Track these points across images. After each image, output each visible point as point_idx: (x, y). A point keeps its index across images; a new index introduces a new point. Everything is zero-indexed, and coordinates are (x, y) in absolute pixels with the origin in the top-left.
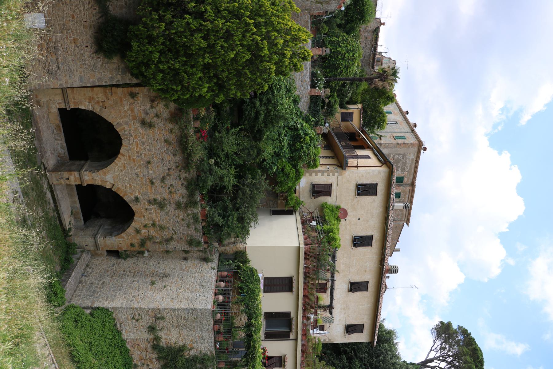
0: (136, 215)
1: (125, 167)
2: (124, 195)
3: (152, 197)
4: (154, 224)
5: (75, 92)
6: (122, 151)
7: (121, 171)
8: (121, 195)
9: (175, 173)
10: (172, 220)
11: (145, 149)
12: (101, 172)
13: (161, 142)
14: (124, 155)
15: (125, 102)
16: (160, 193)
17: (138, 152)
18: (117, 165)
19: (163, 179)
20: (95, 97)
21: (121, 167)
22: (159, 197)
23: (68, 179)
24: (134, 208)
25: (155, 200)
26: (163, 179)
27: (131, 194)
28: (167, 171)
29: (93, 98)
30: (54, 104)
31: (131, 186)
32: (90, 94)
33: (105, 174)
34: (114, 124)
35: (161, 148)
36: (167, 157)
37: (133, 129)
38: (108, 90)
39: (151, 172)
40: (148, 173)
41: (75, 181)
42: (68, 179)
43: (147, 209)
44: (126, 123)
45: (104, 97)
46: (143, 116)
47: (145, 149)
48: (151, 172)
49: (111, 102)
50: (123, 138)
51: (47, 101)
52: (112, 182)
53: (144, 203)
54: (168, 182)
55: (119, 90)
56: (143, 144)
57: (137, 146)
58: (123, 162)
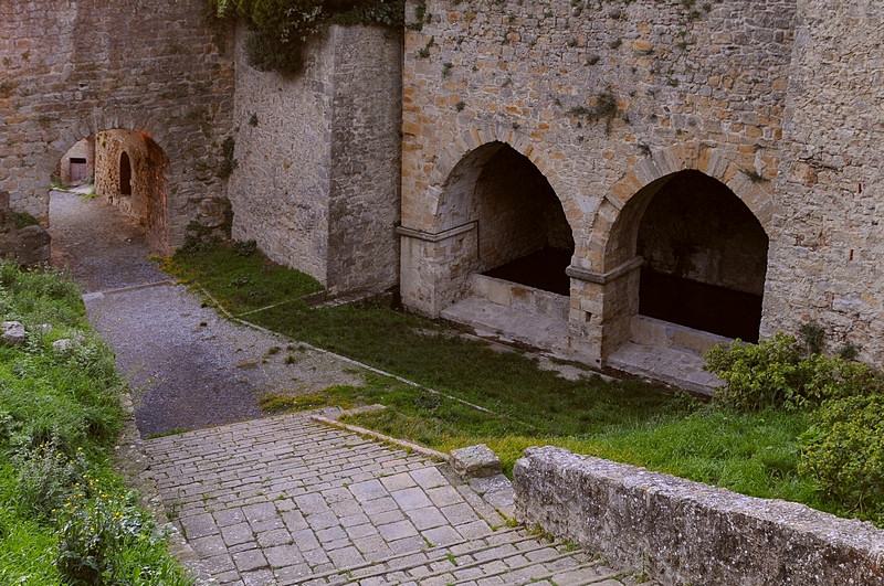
1: (558, 155)
2: (635, 181)
5: (408, 211)
7: (567, 166)
18: (551, 171)
20: (416, 172)
21: (557, 164)
23: (589, 314)
27: (630, 161)
30: (426, 265)
31: (606, 155)
33: (576, 212)
41: (592, 297)
42: (589, 314)
45: (418, 152)
49: (426, 145)
50: (493, 140)
51: (422, 278)
52: (598, 200)
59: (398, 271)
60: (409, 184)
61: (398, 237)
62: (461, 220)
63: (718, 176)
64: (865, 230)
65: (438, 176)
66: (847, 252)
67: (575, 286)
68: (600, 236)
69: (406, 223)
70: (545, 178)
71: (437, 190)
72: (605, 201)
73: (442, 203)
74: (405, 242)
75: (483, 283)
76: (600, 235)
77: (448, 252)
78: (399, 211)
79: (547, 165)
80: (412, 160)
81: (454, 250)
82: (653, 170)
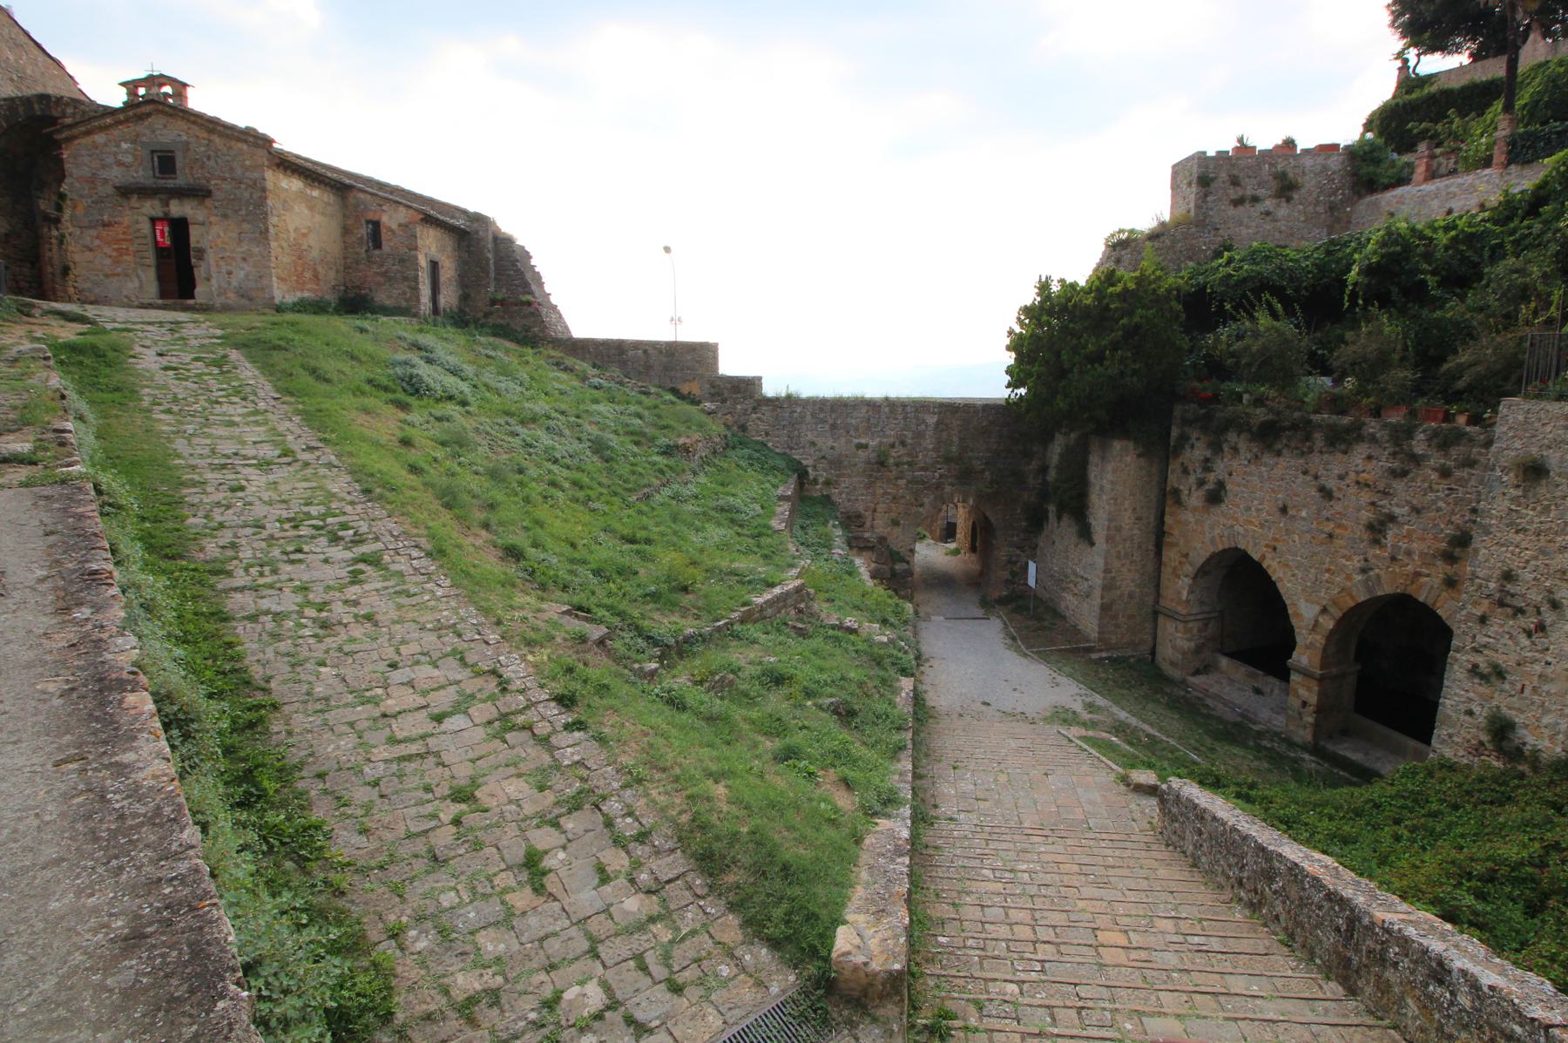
0: (1411, 590)
1: (1287, 565)
2: (1352, 597)
3: (1360, 532)
4: (1450, 558)
6: (1256, 557)
8: (1352, 604)
9: (1316, 462)
10: (1441, 504)
11: (1258, 510)
12: (1294, 621)
13: (1250, 474)
14: (1263, 557)
15: (1183, 517)
16: (1356, 507)
17: (1262, 526)
19: (1326, 494)
22: (1366, 515)
24: (1386, 589)
25: (1370, 527)
26: (1326, 494)
27: (1349, 577)
28: (1308, 478)
29: (1175, 569)
31: (1328, 570)
32: (1169, 570)
33: (1298, 615)
34: (1212, 549)
35: (1261, 476)
36: (1278, 472)
37: (1222, 520)
38: (1167, 539)
39: (1304, 514)
40: (1304, 519)
41: (1309, 689)
43: (1393, 559)
44: (1212, 527)
46: (1201, 493)
47: (1258, 510)
48: (1304, 514)
49: (1182, 542)
52: (1317, 609)
53: (1376, 556)
54: (1331, 484)
55: (1168, 519)
56: (1248, 509)
57: (1251, 523)
58: (1275, 564)
59: (1155, 638)
60: (1166, 572)
61: (1156, 613)
62: (1206, 609)
63: (1430, 602)
64: (1538, 668)
65: (1189, 569)
66: (1519, 686)
67: (1294, 677)
68: (1319, 640)
69: (1162, 602)
70: (1274, 584)
71: (1188, 581)
72: (1324, 610)
73: (1191, 592)
74: (1161, 619)
75: (1224, 662)
76: (1318, 637)
77: (1195, 631)
78: (1158, 594)
79: (1273, 566)
80: (1170, 555)
81: (1200, 630)
82: (1369, 590)
